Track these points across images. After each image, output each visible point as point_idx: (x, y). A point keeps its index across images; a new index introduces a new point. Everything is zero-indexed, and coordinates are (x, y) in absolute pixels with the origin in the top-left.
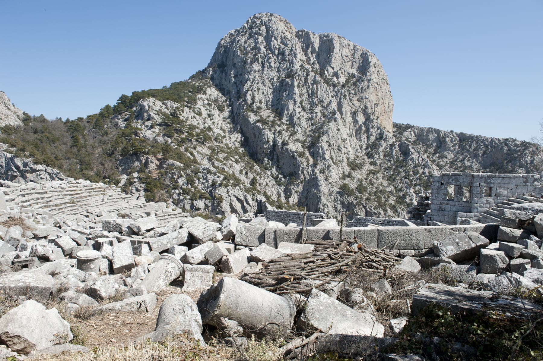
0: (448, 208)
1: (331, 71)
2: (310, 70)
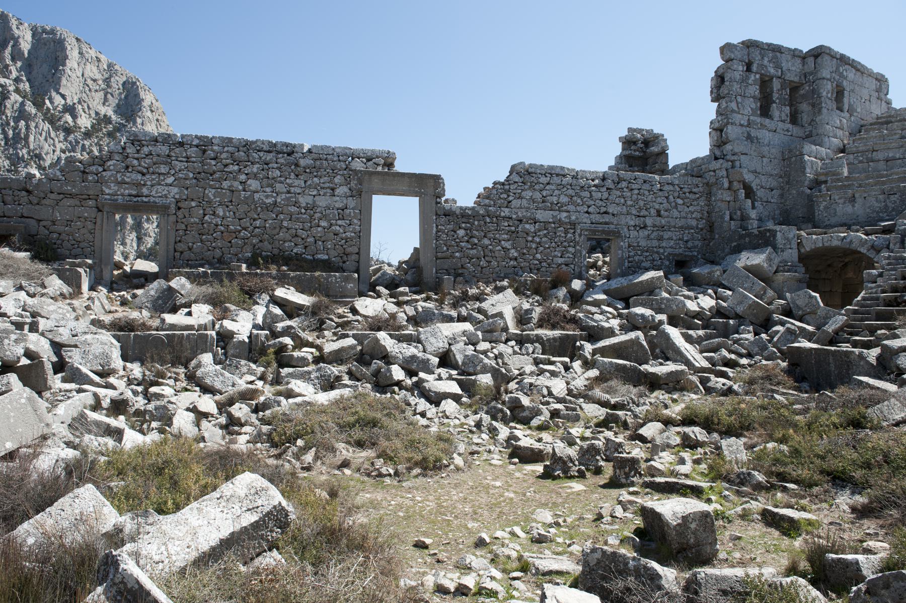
0: (765, 135)
1: (58, 100)
2: (12, 88)
